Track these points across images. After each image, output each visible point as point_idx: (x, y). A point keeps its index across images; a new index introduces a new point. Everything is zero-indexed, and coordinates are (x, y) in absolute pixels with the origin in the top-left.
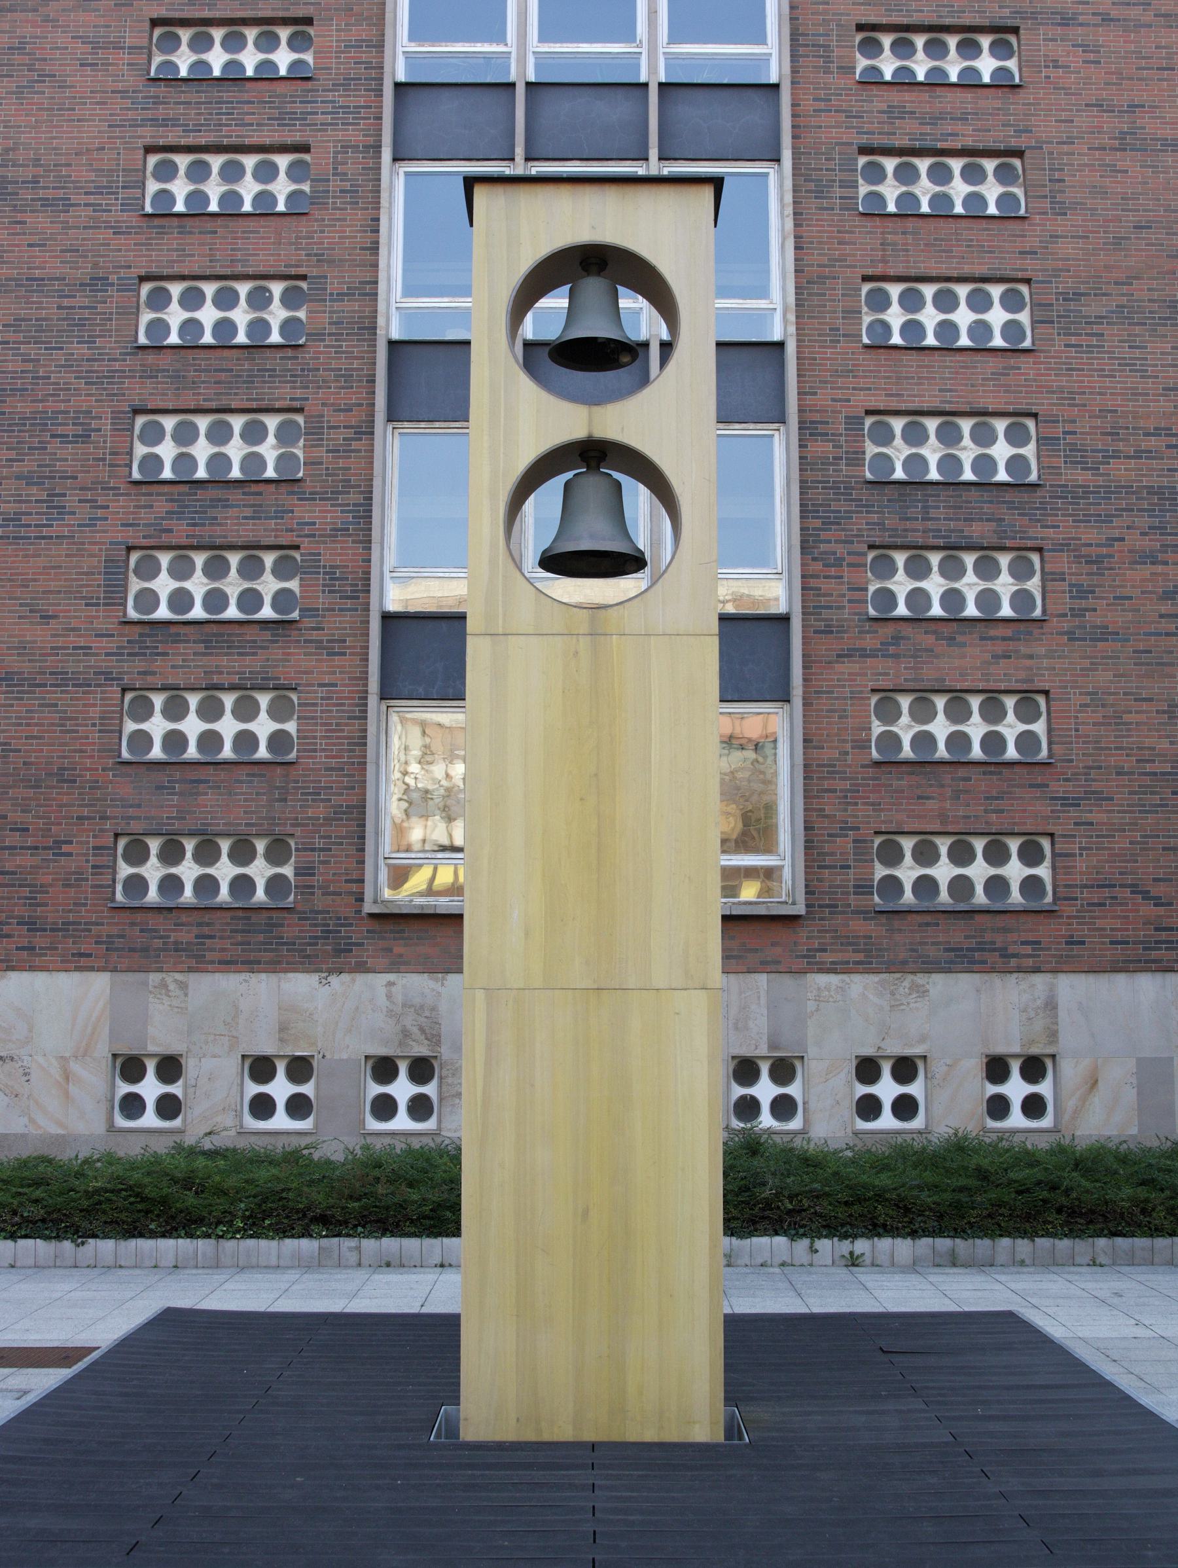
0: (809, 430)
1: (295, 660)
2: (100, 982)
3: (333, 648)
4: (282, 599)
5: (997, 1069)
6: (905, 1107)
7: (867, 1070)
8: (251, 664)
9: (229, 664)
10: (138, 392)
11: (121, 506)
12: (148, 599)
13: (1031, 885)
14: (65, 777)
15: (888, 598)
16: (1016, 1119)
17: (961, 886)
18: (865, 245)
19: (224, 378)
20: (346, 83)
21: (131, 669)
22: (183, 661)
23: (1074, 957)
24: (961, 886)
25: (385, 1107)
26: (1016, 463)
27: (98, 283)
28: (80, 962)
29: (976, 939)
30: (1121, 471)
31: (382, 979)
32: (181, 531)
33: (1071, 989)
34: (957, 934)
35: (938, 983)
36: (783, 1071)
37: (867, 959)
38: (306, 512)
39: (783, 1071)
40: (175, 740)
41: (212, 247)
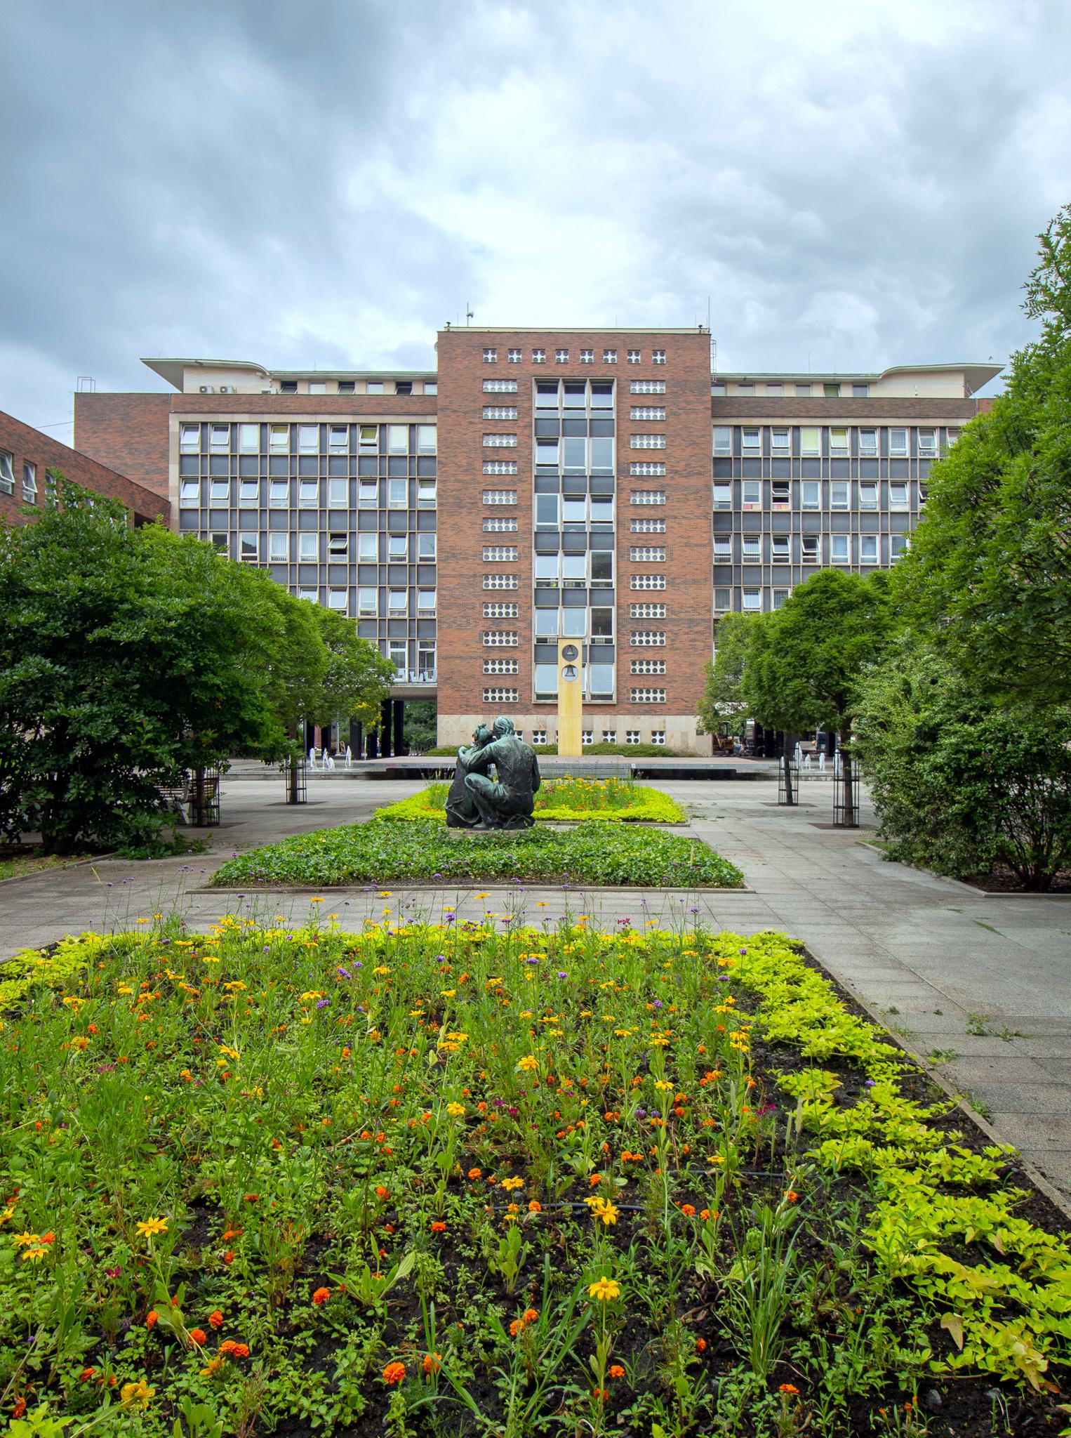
0: (619, 607)
1: (517, 655)
2: (481, 717)
3: (525, 652)
4: (514, 641)
5: (654, 733)
6: (636, 741)
7: (629, 733)
8: (508, 655)
9: (505, 655)
10: (484, 599)
11: (481, 623)
12: (487, 641)
13: (662, 699)
14: (472, 677)
15: (634, 642)
16: (658, 743)
17: (648, 698)
18: (631, 569)
19: (502, 597)
20: (524, 532)
21: (485, 656)
22: (495, 655)
23: (669, 712)
24: (648, 698)
25: (536, 740)
26: (662, 614)
27: (475, 576)
28: (477, 713)
29: (651, 709)
30: (682, 615)
31: (534, 717)
32: (494, 628)
33: (669, 718)
34: (646, 708)
35: (643, 717)
36: (613, 733)
37: (629, 713)
38: (518, 624)
39: (613, 733)
40: (494, 670)
41: (498, 570)
